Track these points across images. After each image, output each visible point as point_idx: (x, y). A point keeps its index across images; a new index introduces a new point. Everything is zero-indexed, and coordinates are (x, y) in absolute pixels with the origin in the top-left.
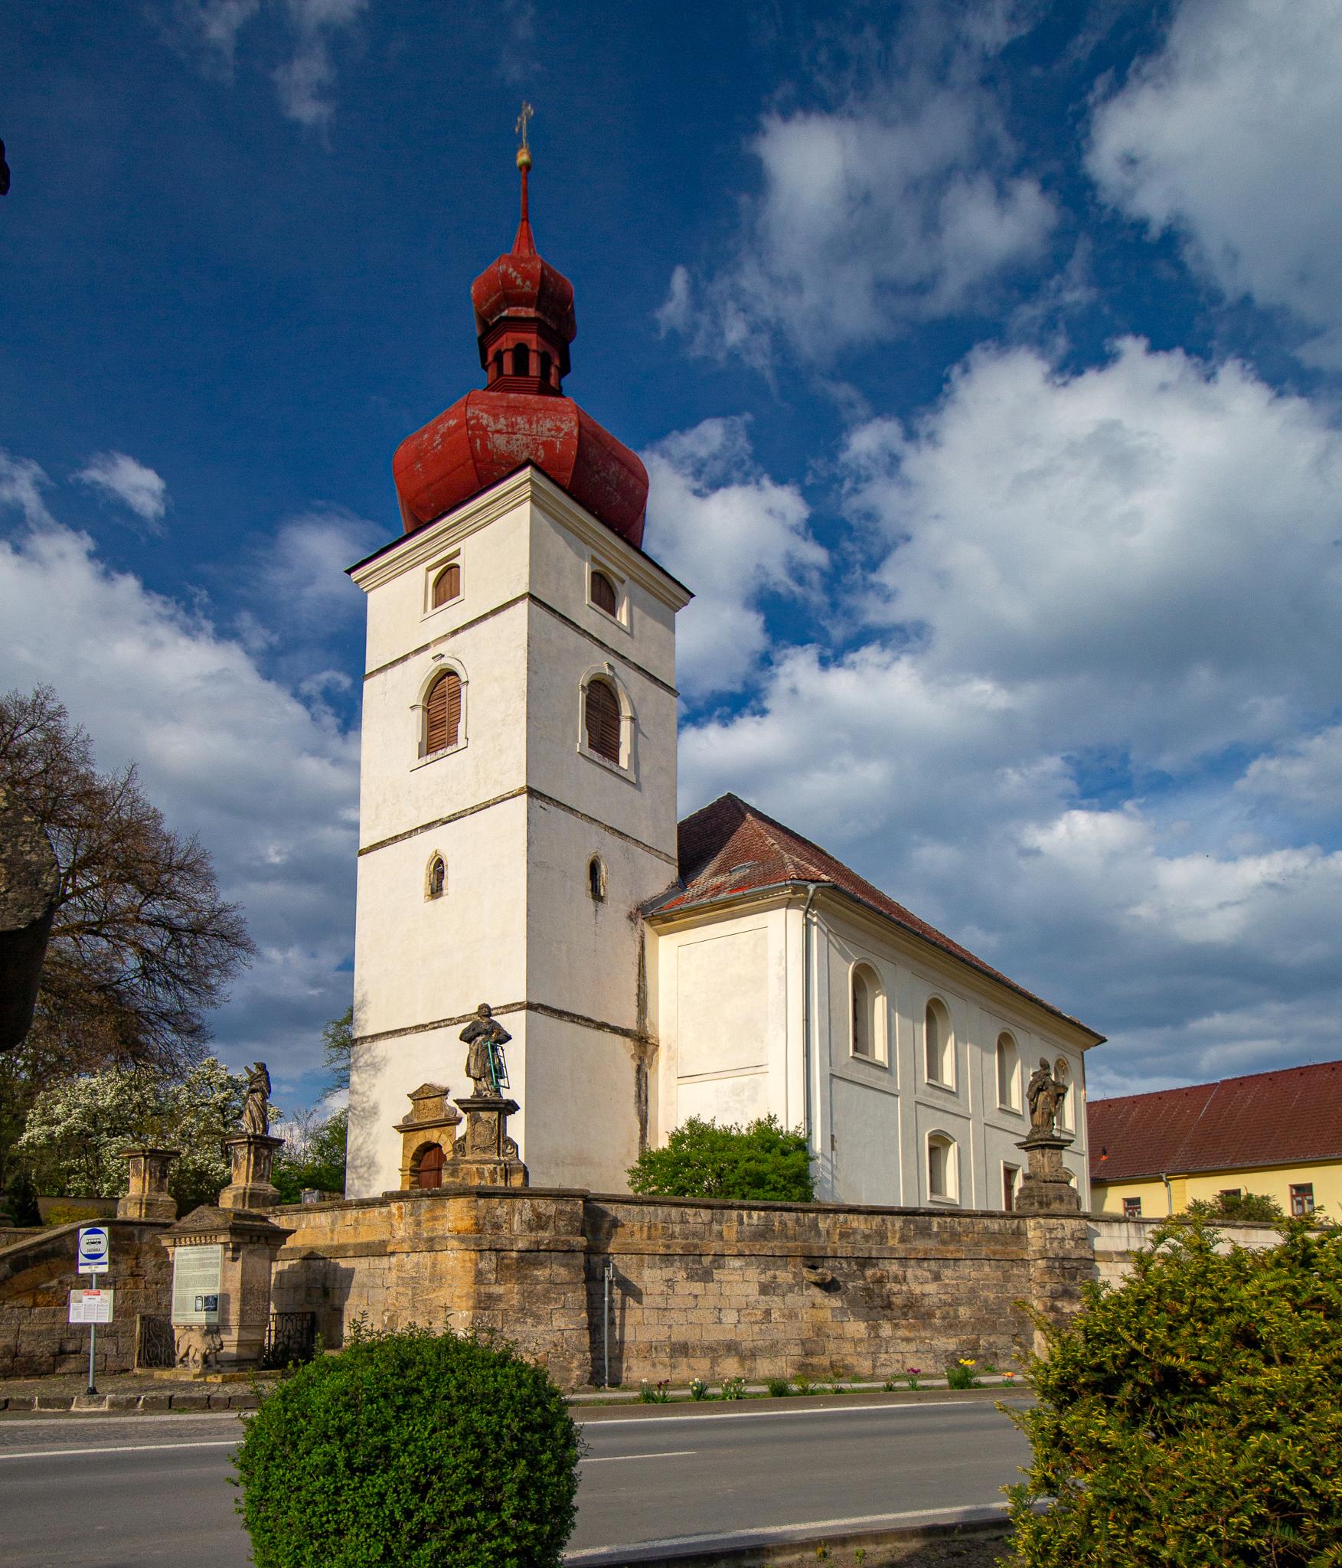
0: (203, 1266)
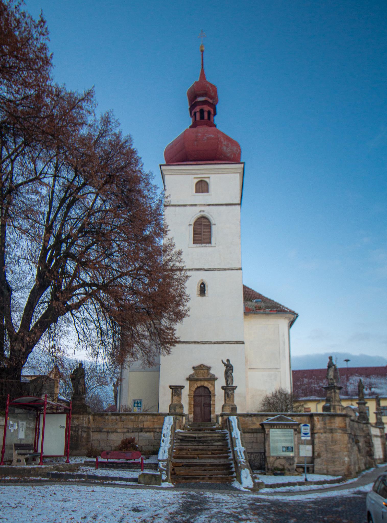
0: (285, 436)
